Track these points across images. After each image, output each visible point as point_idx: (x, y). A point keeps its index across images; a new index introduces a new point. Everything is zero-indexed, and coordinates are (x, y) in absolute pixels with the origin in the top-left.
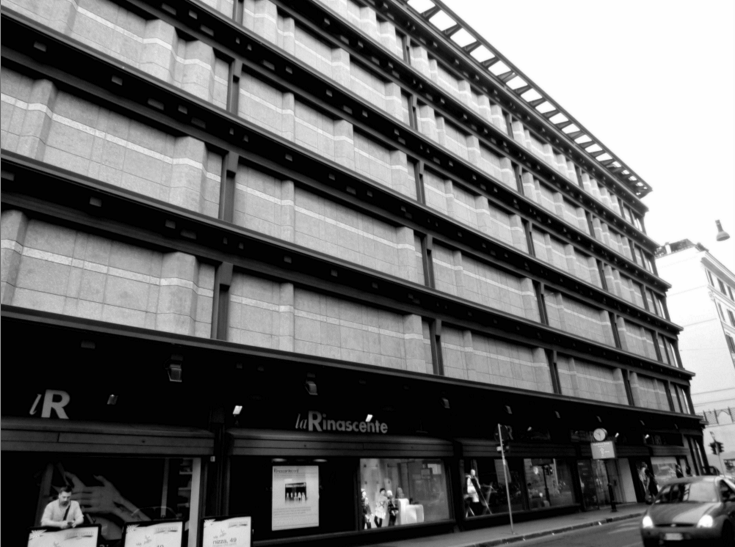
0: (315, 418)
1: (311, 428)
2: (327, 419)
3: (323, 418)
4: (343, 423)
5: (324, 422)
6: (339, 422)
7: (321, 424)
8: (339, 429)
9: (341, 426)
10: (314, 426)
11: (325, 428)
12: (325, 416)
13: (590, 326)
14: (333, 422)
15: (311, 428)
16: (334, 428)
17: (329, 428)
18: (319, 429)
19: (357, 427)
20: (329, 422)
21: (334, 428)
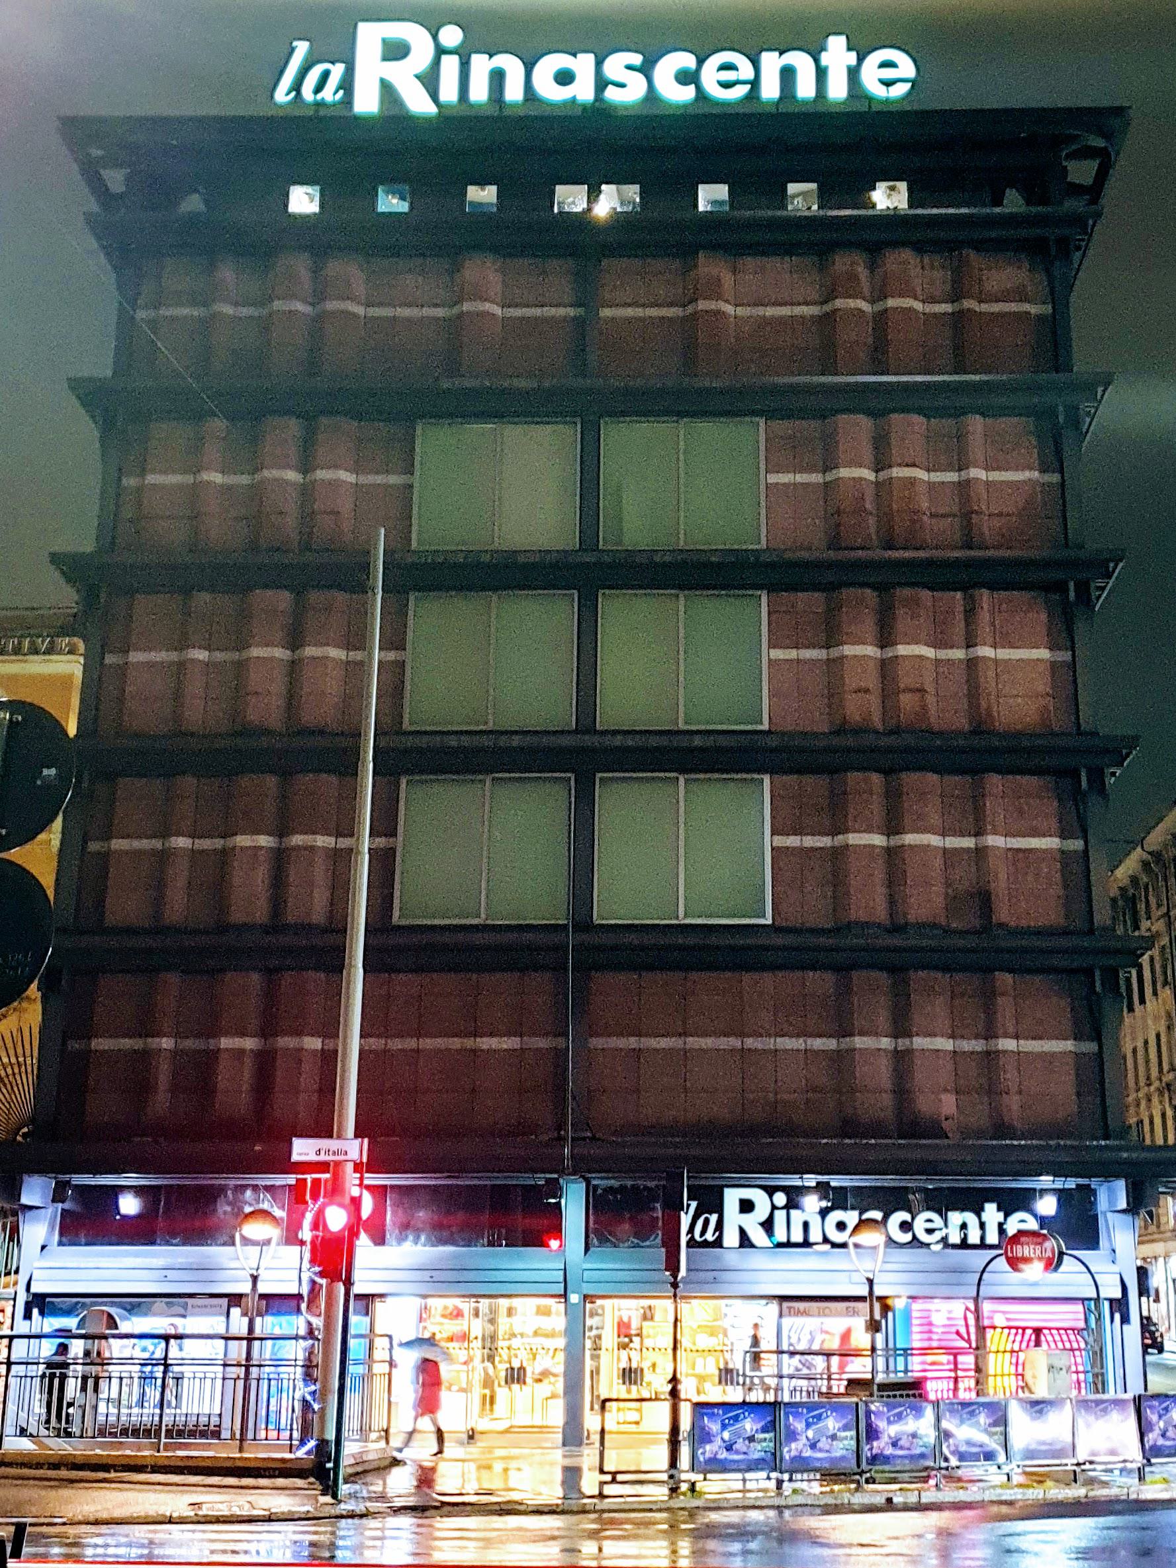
0: (747, 1206)
7: (768, 1225)
10: (743, 1232)
11: (780, 1235)
17: (797, 1237)
19: (906, 1226)
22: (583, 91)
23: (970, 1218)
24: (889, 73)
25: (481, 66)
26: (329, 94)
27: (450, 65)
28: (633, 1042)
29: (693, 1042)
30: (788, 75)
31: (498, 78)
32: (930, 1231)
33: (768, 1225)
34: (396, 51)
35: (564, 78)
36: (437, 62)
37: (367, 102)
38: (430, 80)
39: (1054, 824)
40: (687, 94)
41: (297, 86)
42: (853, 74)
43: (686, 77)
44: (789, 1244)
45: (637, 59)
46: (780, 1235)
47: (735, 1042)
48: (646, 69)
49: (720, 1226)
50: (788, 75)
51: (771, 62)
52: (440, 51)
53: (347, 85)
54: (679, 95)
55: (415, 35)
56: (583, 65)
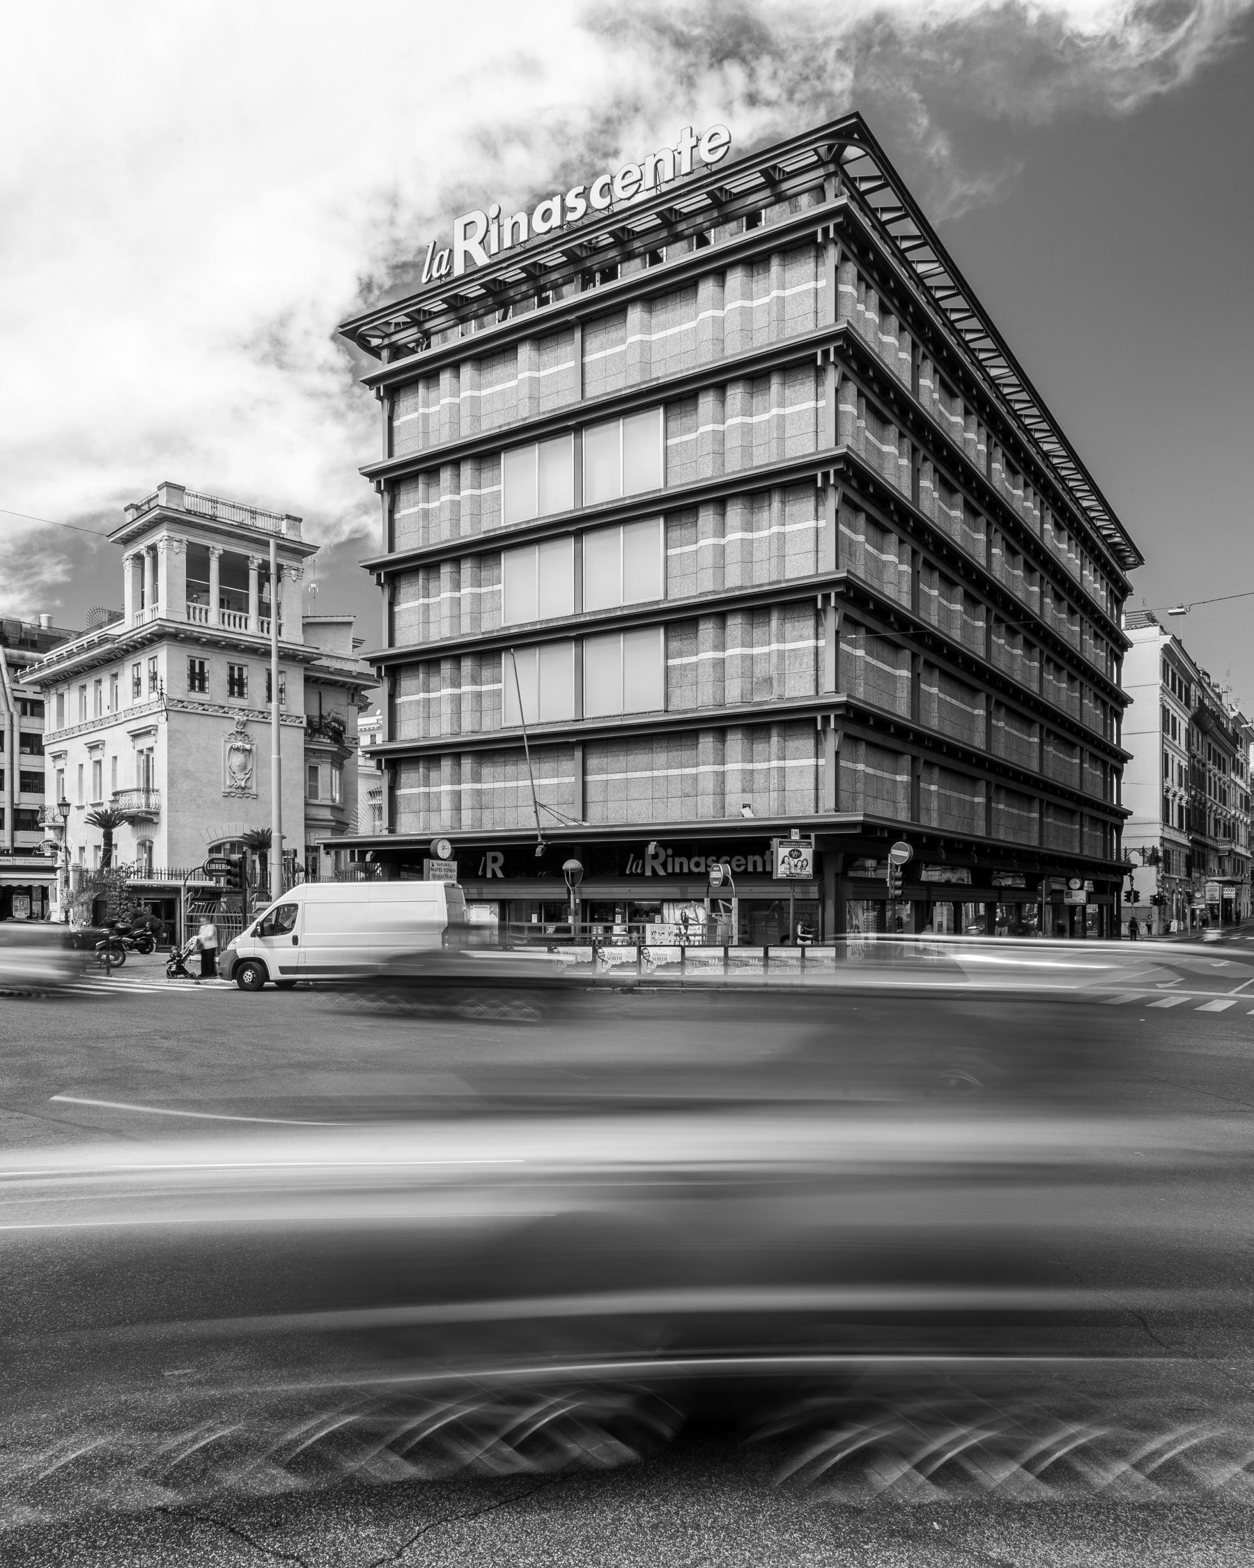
1: (648, 873)
2: (673, 856)
3: (667, 856)
4: (702, 860)
5: (670, 860)
6: (696, 859)
7: (664, 865)
8: (695, 870)
9: (697, 865)
11: (670, 870)
12: (670, 852)
13: (1016, 662)
14: (684, 860)
15: (648, 873)
16: (686, 870)
17: (677, 870)
18: (662, 873)
20: (678, 860)
21: (686, 870)
22: (555, 221)
23: (758, 858)
27: (494, 228)
28: (604, 777)
29: (631, 775)
32: (739, 866)
33: (664, 865)
35: (547, 215)
39: (811, 631)
40: (606, 201)
44: (673, 874)
46: (670, 870)
47: (649, 774)
49: (643, 867)
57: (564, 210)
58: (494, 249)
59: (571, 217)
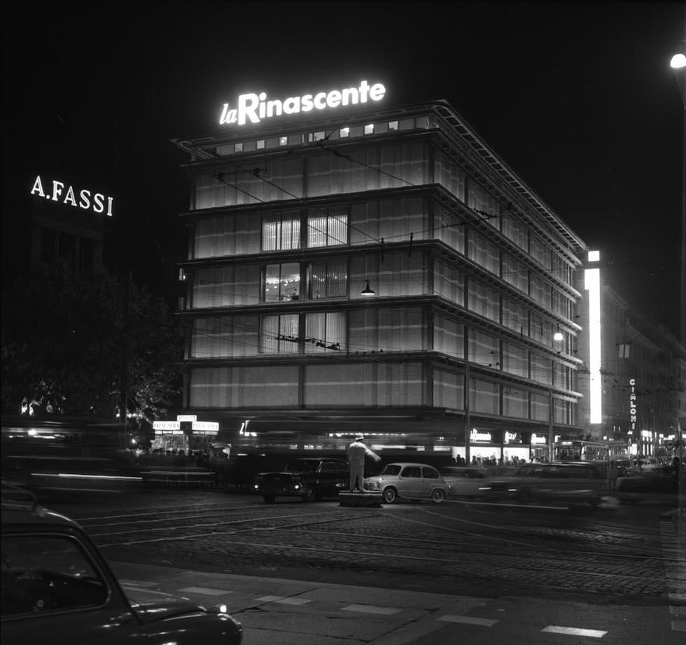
22: (296, 110)
24: (378, 92)
25: (271, 104)
26: (233, 121)
27: (263, 105)
30: (350, 96)
31: (275, 108)
34: (249, 103)
35: (292, 105)
36: (259, 106)
37: (242, 122)
38: (257, 111)
41: (225, 119)
42: (368, 93)
43: (323, 100)
45: (310, 96)
48: (312, 100)
50: (350, 96)
51: (346, 92)
52: (260, 101)
53: (237, 116)
54: (321, 107)
55: (251, 96)
56: (296, 100)
57: (301, 105)
58: (262, 116)
59: (304, 109)
